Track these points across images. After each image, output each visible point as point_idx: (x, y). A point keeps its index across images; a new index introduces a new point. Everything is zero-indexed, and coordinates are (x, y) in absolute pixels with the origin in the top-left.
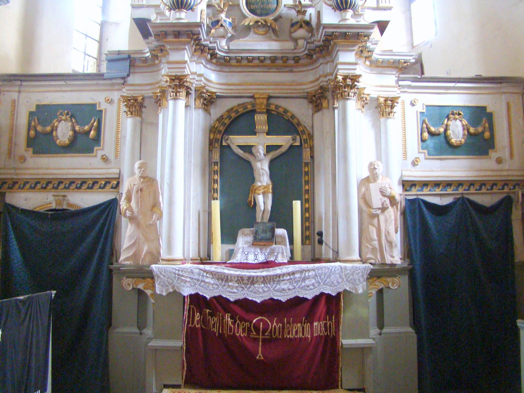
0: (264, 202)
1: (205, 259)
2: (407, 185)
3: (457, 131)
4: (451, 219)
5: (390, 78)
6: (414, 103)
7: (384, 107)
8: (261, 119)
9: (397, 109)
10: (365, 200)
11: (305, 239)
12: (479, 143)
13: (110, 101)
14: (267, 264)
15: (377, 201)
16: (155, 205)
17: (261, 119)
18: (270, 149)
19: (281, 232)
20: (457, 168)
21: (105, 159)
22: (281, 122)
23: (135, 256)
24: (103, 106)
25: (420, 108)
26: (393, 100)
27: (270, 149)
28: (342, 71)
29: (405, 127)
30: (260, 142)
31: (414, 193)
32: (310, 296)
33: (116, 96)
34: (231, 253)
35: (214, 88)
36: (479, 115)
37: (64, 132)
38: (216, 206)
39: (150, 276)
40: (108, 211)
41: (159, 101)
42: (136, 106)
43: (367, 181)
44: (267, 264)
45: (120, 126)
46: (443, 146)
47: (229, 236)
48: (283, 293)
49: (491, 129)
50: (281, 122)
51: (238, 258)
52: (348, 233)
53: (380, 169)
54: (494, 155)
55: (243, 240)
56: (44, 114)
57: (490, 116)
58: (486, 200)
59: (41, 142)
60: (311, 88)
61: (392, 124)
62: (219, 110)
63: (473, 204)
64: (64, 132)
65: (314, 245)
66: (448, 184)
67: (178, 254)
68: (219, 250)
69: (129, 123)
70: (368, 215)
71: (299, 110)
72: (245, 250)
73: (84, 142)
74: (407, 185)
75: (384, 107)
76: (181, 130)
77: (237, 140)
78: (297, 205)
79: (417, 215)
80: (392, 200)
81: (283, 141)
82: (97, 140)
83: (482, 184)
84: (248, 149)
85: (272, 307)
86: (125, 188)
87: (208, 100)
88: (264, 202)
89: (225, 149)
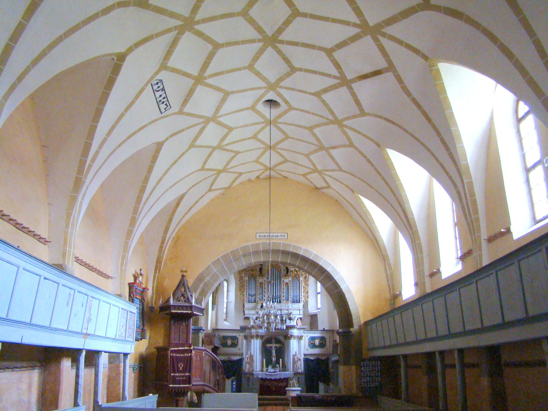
0: (274, 359)
1: (262, 371)
2: (305, 355)
3: (317, 342)
4: (315, 362)
5: (302, 331)
6: (307, 336)
7: (300, 338)
8: (273, 340)
9: (303, 338)
10: (294, 359)
11: (282, 367)
12: (322, 345)
13: (240, 336)
14: (275, 372)
15: (296, 359)
16: (253, 360)
17: (273, 340)
18: (275, 347)
19: (277, 365)
20: (316, 351)
21: (239, 349)
22: (278, 341)
23: (249, 371)
24: (238, 337)
25: (309, 337)
26: (302, 336)
27: (275, 347)
28: (290, 334)
29: (305, 342)
30: (273, 345)
31: (306, 357)
32: (283, 378)
33: (241, 334)
34: (267, 370)
35: (263, 334)
36: (322, 339)
37: (229, 342)
38: (264, 360)
39: (252, 374)
40: (240, 361)
41: (252, 337)
42: (246, 337)
43: (295, 355)
44: (275, 372)
45: (242, 342)
46: (313, 346)
47: (267, 366)
48: (278, 377)
49: (325, 342)
50: (278, 341)
51: (269, 371)
52: (290, 366)
53: (297, 353)
54: (326, 348)
55: (270, 367)
56: (225, 338)
57: (325, 339)
58: (323, 358)
59: (225, 345)
60: (284, 334)
61: (302, 342)
62: (264, 339)
63: (320, 359)
64: (229, 342)
65: (284, 368)
66: (315, 355)
67: (258, 370)
68: (265, 369)
69: (245, 341)
70: (294, 362)
71: (281, 338)
72: (270, 369)
73: (234, 345)
74: (305, 355)
75: (300, 338)
76: (256, 345)
77: (268, 345)
78: (281, 360)
79: (306, 361)
80: (300, 360)
81: (278, 345)
82: (237, 344)
83: (322, 355)
84: (271, 347)
85: (275, 380)
86: (244, 356)
87: (262, 337)
88: (274, 359)
89: (266, 348)
